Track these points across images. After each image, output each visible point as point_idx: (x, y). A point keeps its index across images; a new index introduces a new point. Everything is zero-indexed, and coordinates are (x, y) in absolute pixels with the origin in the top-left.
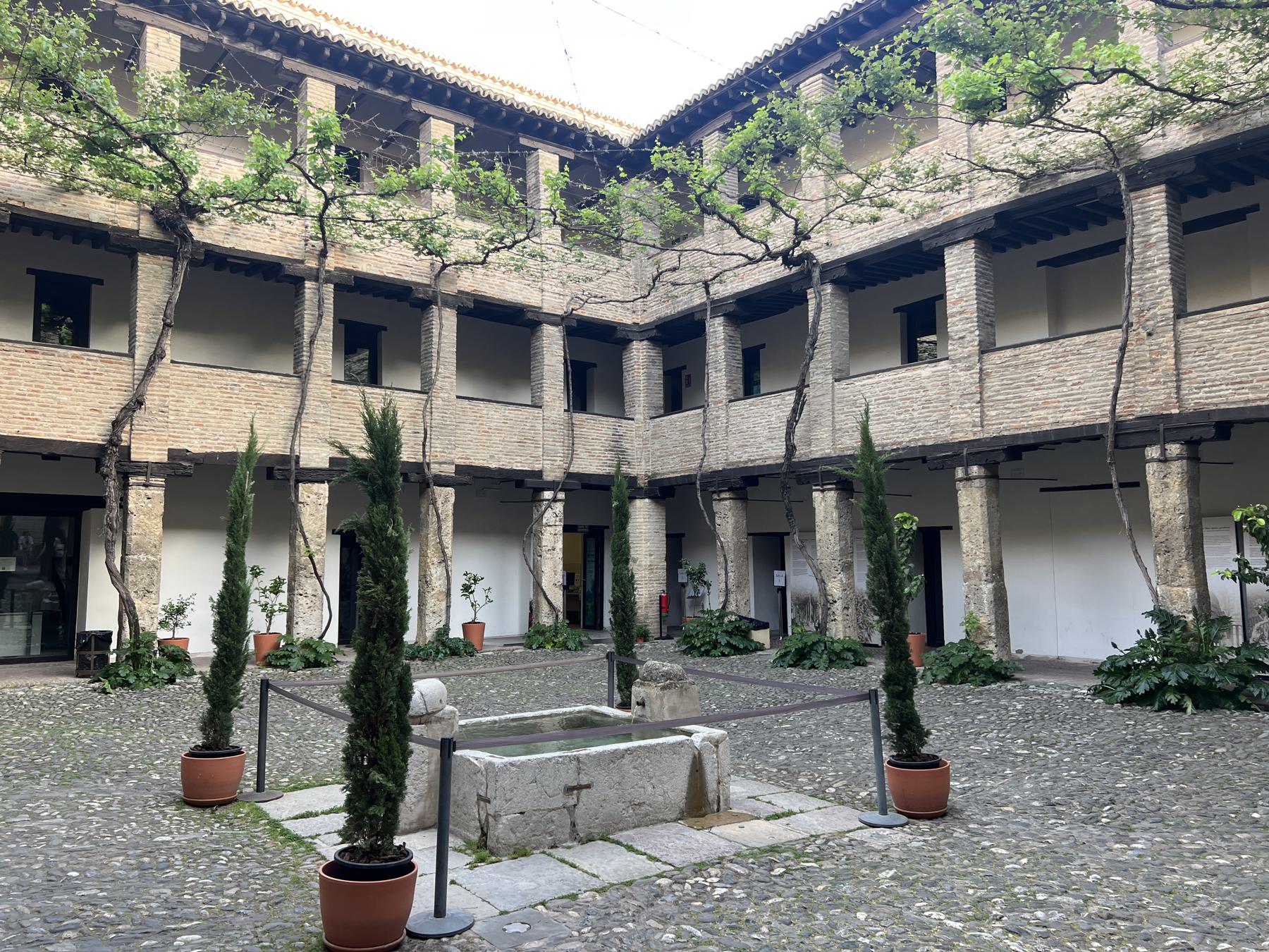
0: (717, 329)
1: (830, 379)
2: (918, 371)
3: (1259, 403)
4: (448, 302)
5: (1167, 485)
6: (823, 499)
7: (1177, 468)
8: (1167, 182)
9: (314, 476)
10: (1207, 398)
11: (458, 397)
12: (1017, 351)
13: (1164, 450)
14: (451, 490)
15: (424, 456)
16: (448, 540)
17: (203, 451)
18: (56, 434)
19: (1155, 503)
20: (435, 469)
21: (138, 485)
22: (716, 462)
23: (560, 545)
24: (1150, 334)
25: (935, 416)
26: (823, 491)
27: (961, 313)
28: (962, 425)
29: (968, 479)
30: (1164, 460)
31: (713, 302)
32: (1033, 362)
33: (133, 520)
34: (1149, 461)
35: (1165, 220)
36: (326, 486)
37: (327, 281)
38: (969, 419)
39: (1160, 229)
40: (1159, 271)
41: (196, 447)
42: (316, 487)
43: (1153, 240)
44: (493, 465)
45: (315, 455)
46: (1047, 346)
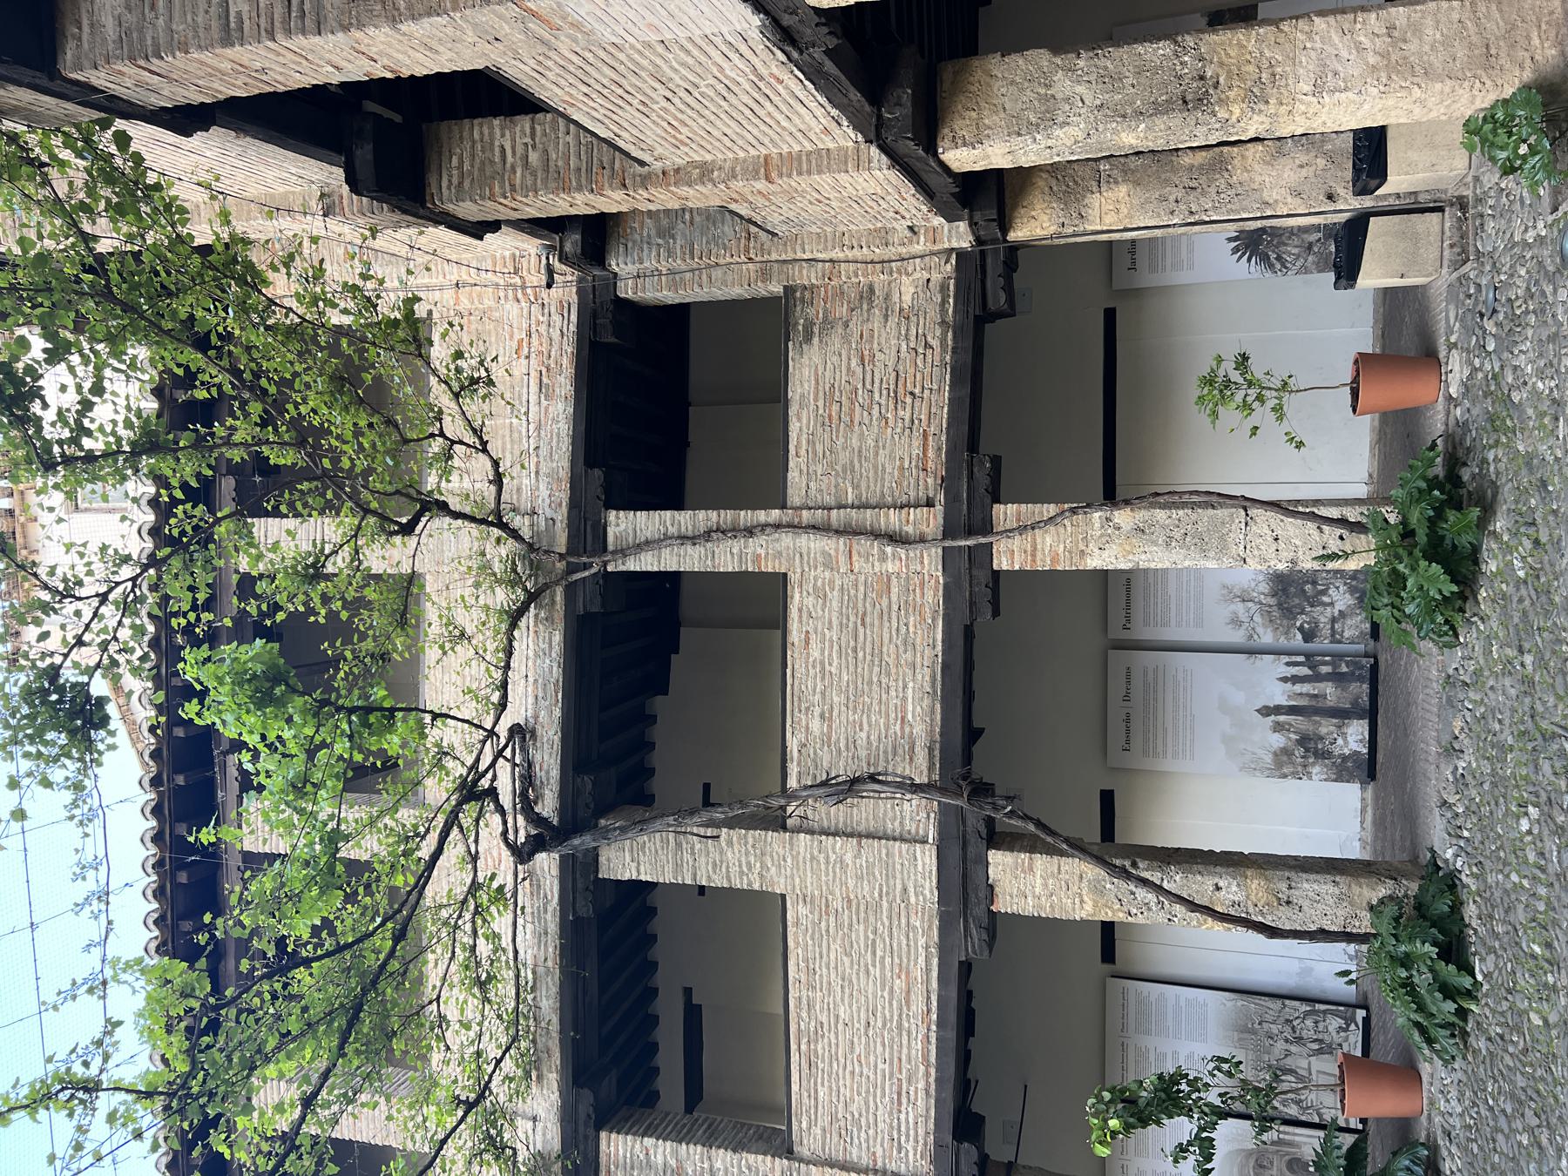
3: (932, 1080)
8: (598, 1129)
10: (917, 1142)
35: (649, 1142)
39: (660, 1150)
40: (718, 1165)
43: (673, 1162)
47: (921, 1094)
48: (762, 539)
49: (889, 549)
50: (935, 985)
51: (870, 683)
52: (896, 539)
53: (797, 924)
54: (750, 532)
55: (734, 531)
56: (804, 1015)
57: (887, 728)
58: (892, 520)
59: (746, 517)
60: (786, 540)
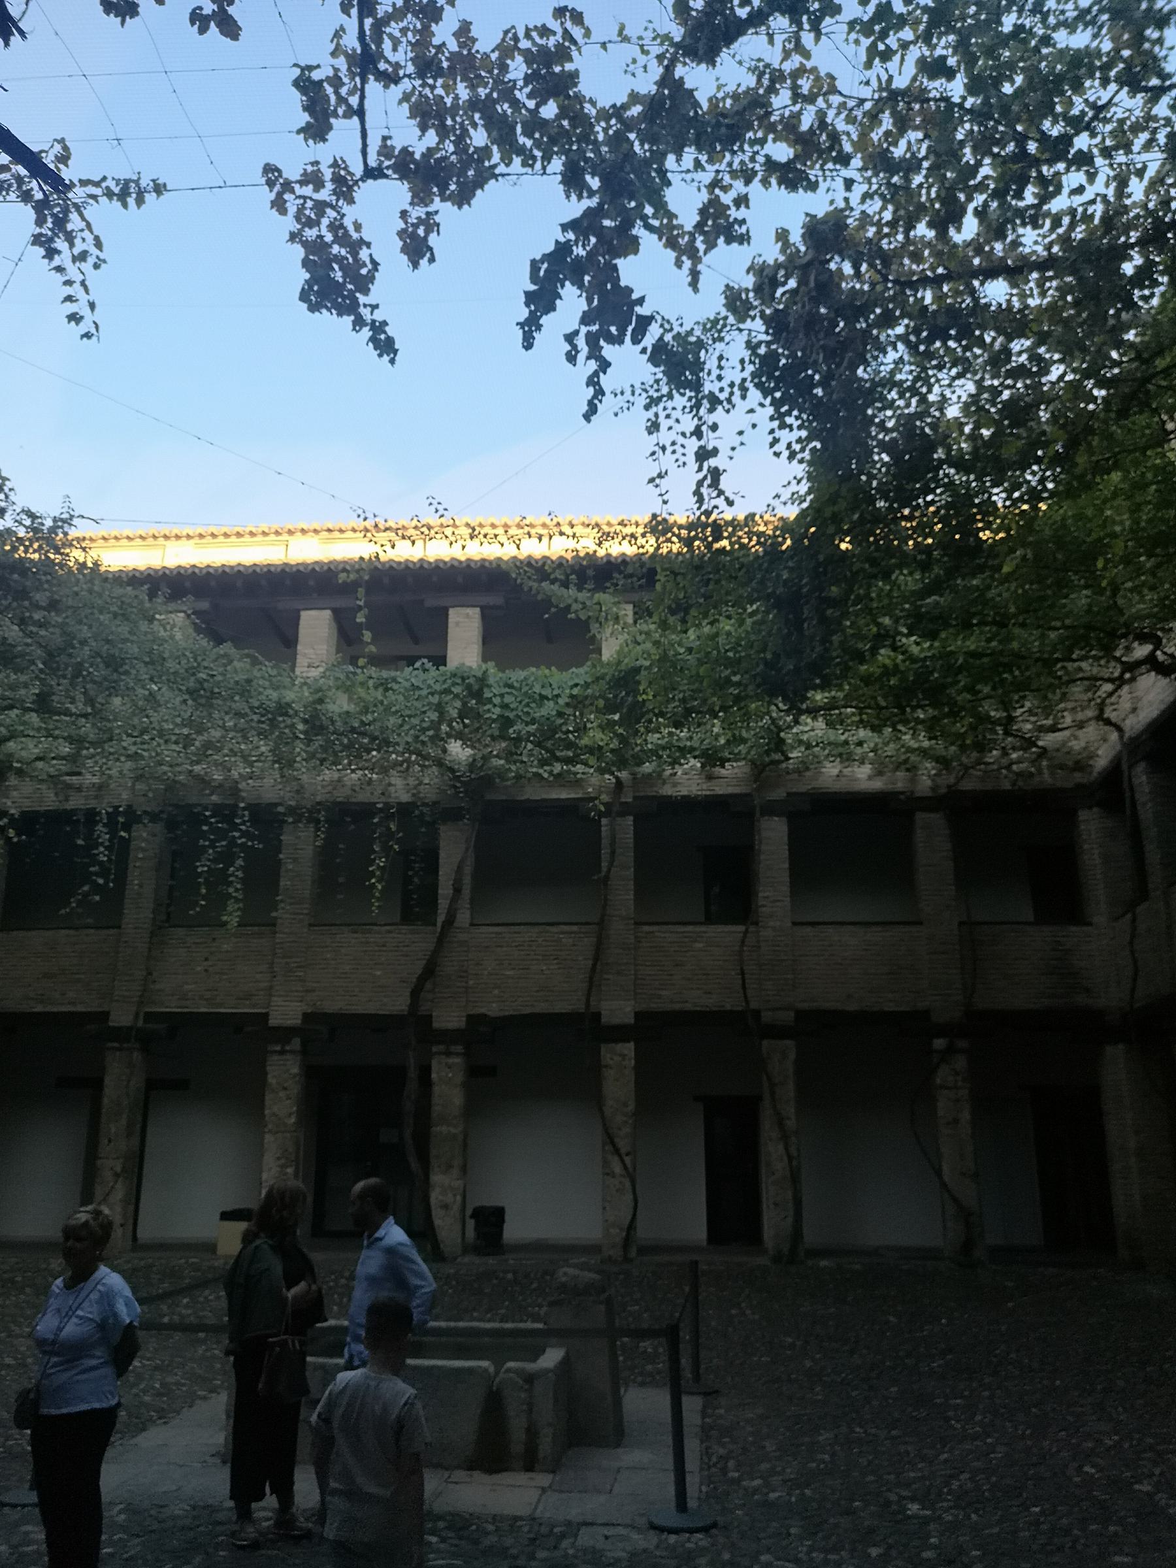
0: (1141, 777)
4: (771, 809)
9: (619, 1033)
11: (794, 924)
14: (790, 1043)
15: (747, 1002)
16: (790, 1110)
17: (502, 1014)
18: (371, 1008)
20: (767, 1017)
21: (440, 1053)
23: (966, 1116)
33: (436, 1090)
36: (632, 1045)
37: (622, 814)
41: (493, 1009)
42: (619, 1047)
44: (852, 1007)
45: (618, 1009)
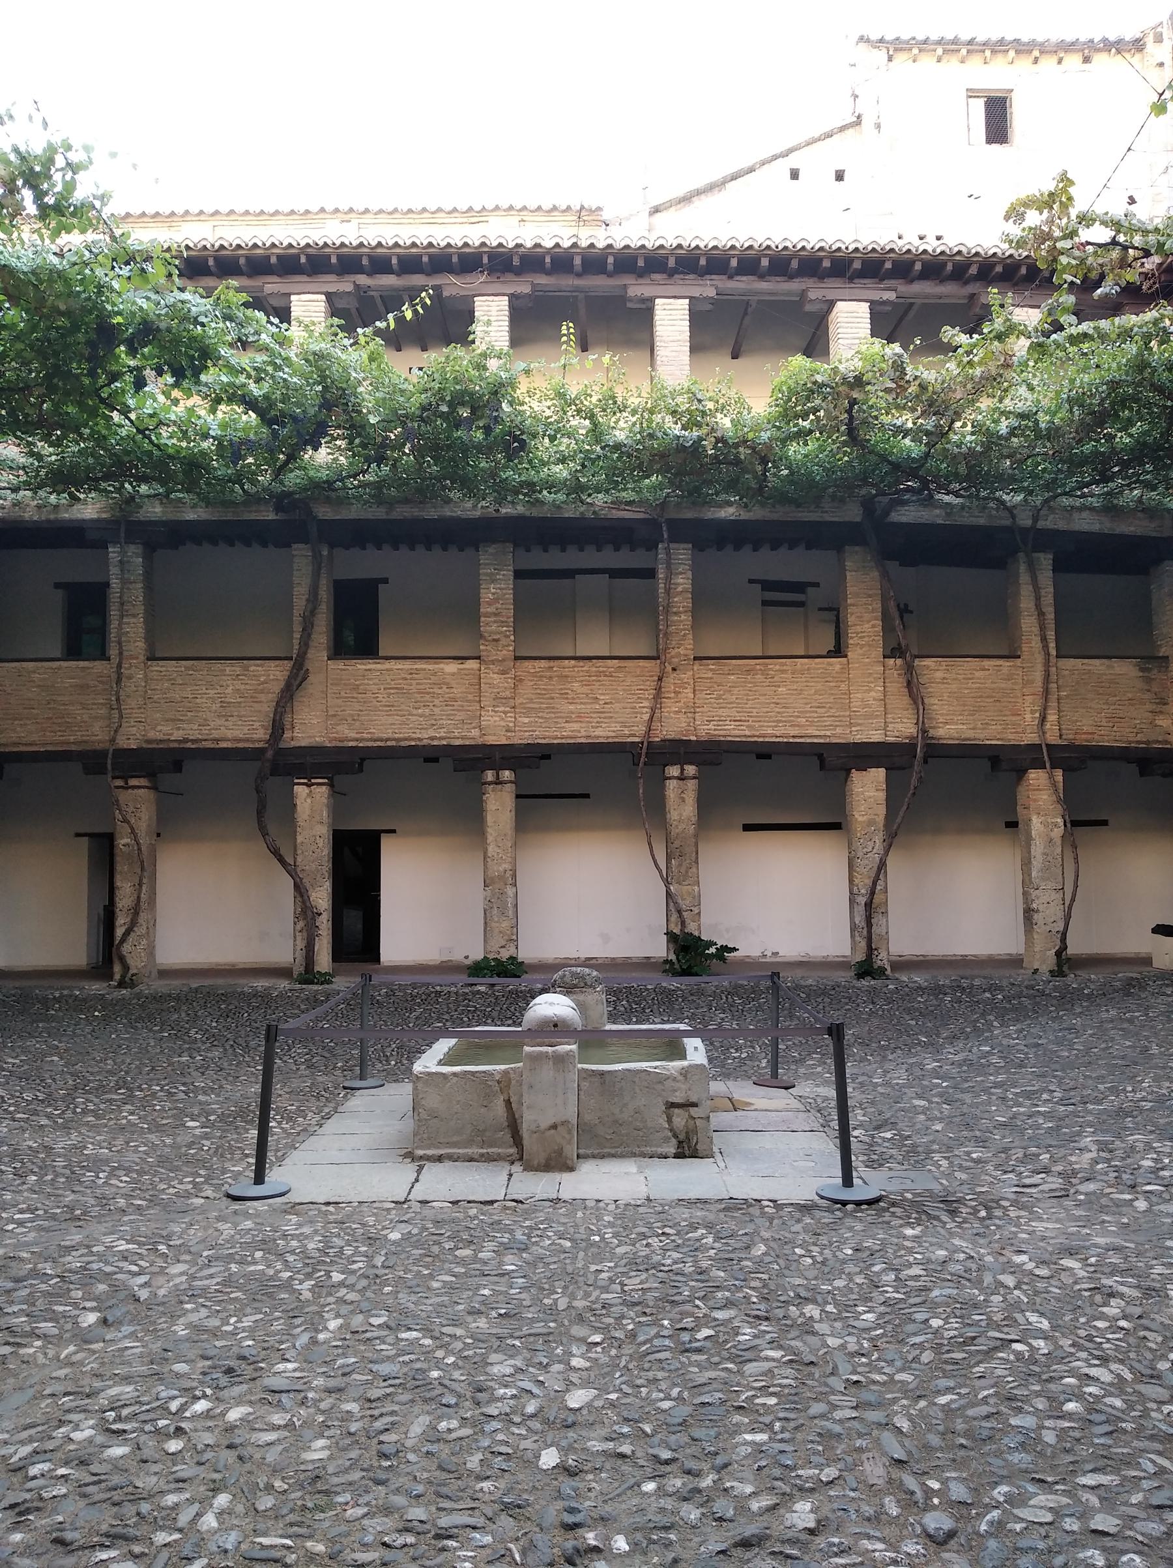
1: (325, 655)
2: (441, 666)
5: (683, 800)
6: (310, 795)
7: (692, 785)
12: (552, 663)
13: (682, 770)
19: (673, 815)
22: (131, 737)
24: (674, 669)
25: (461, 716)
26: (309, 786)
27: (496, 615)
28: (498, 726)
29: (498, 782)
30: (681, 778)
31: (130, 523)
32: (566, 676)
34: (670, 778)
35: (690, 574)
38: (503, 723)
43: (680, 589)
46: (581, 664)
47: (742, 733)
48: (1040, 645)
49: (1037, 715)
50: (809, 741)
51: (964, 705)
52: (1043, 719)
53: (829, 664)
54: (1044, 639)
55: (1042, 628)
56: (778, 667)
57: (942, 715)
58: (1052, 717)
59: (1051, 635)
60: (1039, 659)
